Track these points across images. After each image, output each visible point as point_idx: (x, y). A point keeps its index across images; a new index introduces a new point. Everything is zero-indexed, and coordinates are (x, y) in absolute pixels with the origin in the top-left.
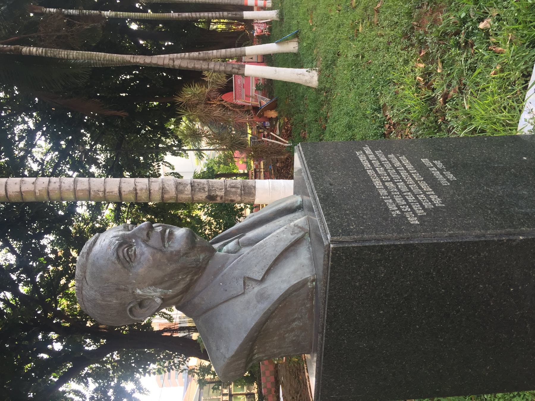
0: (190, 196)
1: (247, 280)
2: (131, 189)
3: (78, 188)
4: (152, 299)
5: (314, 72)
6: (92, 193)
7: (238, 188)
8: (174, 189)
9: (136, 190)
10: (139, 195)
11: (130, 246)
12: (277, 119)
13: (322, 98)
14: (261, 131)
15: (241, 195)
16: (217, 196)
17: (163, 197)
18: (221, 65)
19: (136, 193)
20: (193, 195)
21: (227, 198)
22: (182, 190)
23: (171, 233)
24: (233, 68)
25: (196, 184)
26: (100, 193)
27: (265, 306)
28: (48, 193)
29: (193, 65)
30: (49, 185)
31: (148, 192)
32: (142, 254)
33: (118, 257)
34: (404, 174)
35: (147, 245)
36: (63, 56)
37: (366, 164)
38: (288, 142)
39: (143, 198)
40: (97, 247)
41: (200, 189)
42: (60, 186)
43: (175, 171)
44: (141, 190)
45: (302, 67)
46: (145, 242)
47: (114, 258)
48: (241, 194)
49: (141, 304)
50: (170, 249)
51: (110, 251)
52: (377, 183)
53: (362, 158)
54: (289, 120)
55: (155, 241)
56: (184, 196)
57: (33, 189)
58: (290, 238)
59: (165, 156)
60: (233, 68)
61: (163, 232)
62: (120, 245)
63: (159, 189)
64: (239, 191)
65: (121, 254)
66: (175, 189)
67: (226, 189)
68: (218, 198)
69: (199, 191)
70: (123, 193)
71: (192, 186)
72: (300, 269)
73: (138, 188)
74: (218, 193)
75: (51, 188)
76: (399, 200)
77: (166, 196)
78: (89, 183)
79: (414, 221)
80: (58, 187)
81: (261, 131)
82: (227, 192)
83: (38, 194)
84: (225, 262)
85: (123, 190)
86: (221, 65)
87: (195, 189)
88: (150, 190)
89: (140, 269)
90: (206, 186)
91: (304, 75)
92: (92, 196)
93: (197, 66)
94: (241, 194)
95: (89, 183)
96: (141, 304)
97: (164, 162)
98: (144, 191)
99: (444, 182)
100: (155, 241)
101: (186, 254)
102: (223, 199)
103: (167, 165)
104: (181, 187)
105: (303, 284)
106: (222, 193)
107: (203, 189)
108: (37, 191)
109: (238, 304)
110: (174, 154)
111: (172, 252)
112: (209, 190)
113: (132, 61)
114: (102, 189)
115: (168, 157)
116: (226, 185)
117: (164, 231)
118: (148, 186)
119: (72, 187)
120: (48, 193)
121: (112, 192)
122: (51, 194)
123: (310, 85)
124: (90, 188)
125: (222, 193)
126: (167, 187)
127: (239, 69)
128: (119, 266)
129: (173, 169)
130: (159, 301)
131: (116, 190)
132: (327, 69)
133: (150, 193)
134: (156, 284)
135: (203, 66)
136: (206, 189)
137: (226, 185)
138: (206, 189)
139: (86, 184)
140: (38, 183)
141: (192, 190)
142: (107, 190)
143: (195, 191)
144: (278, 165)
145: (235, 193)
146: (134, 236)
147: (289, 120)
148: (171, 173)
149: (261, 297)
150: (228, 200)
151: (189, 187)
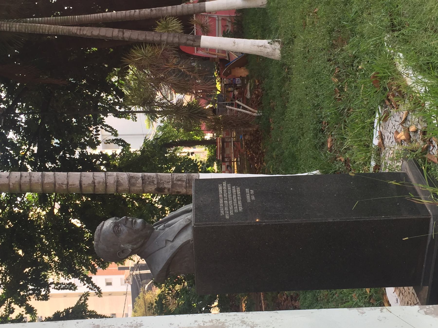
0: (141, 188)
1: (167, 241)
2: (90, 182)
3: (45, 182)
4: (127, 249)
5: (277, 44)
6: (57, 186)
7: (183, 181)
8: (127, 182)
9: (94, 183)
10: (97, 187)
11: (119, 227)
12: (248, 78)
13: (284, 74)
14: (230, 89)
15: (186, 187)
16: (165, 188)
17: (117, 189)
18: (174, 37)
19: (95, 186)
20: (143, 187)
21: (173, 190)
22: (134, 183)
23: (135, 221)
24: (188, 40)
25: (146, 178)
26: (64, 186)
27: (173, 250)
28: (20, 186)
29: (144, 37)
30: (21, 179)
31: (105, 185)
32: (123, 230)
33: (114, 231)
34: (234, 196)
35: (126, 226)
36: (5, 28)
37: (221, 191)
38: (257, 111)
39: (101, 190)
40: (104, 227)
41: (150, 182)
42: (30, 180)
43: (118, 137)
44: (99, 183)
45: (263, 38)
46: (124, 225)
47: (112, 232)
48: (186, 187)
49: (123, 252)
50: (135, 228)
51: (111, 229)
52: (221, 201)
53: (220, 188)
54: (260, 83)
55: (129, 225)
56: (135, 188)
57: (7, 183)
58: (185, 223)
59: (105, 118)
60: (188, 40)
61: (132, 221)
62: (114, 226)
63: (114, 182)
64: (184, 183)
65: (115, 230)
66: (128, 182)
67: (173, 182)
68: (166, 190)
69: (149, 184)
70: (83, 186)
71: (143, 180)
72: (187, 236)
73: (96, 181)
74: (166, 186)
75: (22, 181)
76: (226, 209)
77: (120, 188)
78: (55, 177)
79: (227, 217)
80: (29, 181)
81: (230, 89)
82: (173, 185)
83: (11, 187)
84: (159, 233)
85: (83, 182)
86: (174, 37)
87: (146, 182)
88: (106, 183)
89: (123, 236)
90: (155, 180)
91: (265, 47)
92: (57, 188)
93: (148, 38)
94: (186, 187)
95: (55, 177)
96: (123, 252)
97: (103, 125)
98: (101, 184)
99: (249, 201)
100: (129, 225)
101: (142, 230)
102: (170, 191)
103: (108, 129)
104: (133, 181)
105: (188, 242)
106: (169, 186)
107: (153, 182)
108: (11, 184)
109: (163, 251)
110: (118, 115)
111: (136, 229)
112: (158, 183)
113: (78, 33)
114: (66, 183)
115: (110, 120)
116: (172, 179)
117: (132, 221)
118: (105, 179)
119: (40, 181)
120: (20, 186)
121: (74, 185)
122: (22, 187)
123: (272, 57)
124: (55, 182)
125: (169, 186)
126: (121, 181)
127: (194, 41)
128: (114, 235)
129: (116, 135)
130: (130, 250)
131: (77, 183)
132: (287, 45)
133: (106, 185)
134: (129, 242)
135: (155, 38)
136: (155, 182)
137: (172, 179)
138: (155, 182)
139: (52, 177)
140: (12, 177)
141: (143, 183)
142: (70, 183)
143: (145, 184)
144: (247, 137)
145: (181, 186)
146: (120, 222)
147: (260, 83)
148: (113, 140)
149: (172, 247)
150: (174, 192)
151: (140, 180)
